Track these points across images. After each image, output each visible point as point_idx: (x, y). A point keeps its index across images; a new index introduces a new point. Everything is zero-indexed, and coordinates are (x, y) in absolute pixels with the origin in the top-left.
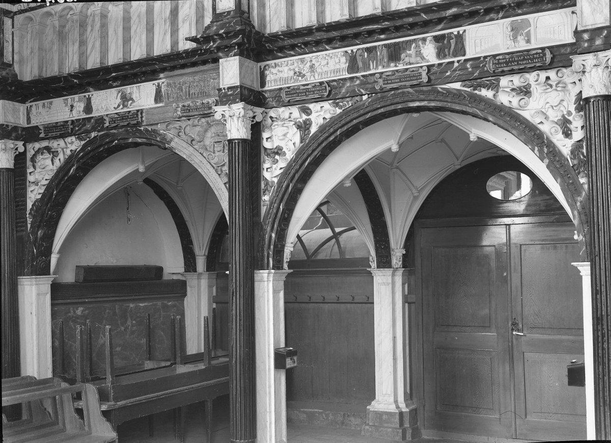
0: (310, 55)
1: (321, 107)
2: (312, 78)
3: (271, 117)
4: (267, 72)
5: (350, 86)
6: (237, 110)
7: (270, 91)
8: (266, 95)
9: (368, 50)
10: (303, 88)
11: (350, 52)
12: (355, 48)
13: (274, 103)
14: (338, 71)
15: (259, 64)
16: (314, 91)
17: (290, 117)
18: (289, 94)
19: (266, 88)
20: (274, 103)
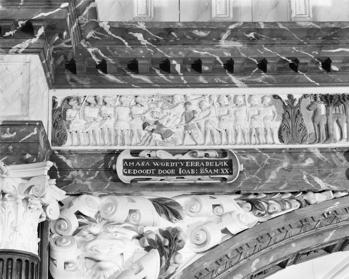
0: (189, 92)
1: (214, 206)
2: (188, 139)
3: (79, 214)
4: (70, 113)
5: (289, 169)
6: (25, 181)
7: (81, 154)
8: (69, 163)
9: (328, 99)
10: (170, 157)
11: (285, 98)
12: (297, 92)
13: (87, 183)
14: (254, 133)
15: (54, 92)
16: (198, 168)
17: (127, 221)
18: (132, 168)
19: (67, 146)
20: (87, 183)
